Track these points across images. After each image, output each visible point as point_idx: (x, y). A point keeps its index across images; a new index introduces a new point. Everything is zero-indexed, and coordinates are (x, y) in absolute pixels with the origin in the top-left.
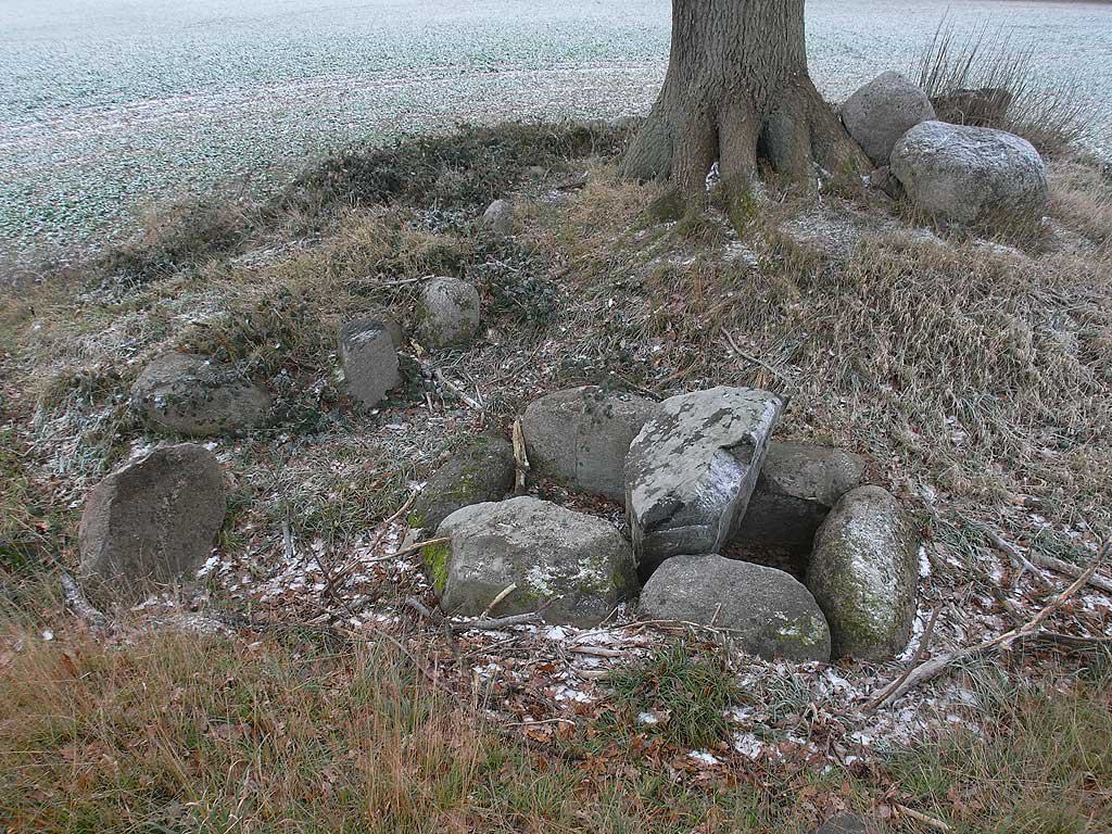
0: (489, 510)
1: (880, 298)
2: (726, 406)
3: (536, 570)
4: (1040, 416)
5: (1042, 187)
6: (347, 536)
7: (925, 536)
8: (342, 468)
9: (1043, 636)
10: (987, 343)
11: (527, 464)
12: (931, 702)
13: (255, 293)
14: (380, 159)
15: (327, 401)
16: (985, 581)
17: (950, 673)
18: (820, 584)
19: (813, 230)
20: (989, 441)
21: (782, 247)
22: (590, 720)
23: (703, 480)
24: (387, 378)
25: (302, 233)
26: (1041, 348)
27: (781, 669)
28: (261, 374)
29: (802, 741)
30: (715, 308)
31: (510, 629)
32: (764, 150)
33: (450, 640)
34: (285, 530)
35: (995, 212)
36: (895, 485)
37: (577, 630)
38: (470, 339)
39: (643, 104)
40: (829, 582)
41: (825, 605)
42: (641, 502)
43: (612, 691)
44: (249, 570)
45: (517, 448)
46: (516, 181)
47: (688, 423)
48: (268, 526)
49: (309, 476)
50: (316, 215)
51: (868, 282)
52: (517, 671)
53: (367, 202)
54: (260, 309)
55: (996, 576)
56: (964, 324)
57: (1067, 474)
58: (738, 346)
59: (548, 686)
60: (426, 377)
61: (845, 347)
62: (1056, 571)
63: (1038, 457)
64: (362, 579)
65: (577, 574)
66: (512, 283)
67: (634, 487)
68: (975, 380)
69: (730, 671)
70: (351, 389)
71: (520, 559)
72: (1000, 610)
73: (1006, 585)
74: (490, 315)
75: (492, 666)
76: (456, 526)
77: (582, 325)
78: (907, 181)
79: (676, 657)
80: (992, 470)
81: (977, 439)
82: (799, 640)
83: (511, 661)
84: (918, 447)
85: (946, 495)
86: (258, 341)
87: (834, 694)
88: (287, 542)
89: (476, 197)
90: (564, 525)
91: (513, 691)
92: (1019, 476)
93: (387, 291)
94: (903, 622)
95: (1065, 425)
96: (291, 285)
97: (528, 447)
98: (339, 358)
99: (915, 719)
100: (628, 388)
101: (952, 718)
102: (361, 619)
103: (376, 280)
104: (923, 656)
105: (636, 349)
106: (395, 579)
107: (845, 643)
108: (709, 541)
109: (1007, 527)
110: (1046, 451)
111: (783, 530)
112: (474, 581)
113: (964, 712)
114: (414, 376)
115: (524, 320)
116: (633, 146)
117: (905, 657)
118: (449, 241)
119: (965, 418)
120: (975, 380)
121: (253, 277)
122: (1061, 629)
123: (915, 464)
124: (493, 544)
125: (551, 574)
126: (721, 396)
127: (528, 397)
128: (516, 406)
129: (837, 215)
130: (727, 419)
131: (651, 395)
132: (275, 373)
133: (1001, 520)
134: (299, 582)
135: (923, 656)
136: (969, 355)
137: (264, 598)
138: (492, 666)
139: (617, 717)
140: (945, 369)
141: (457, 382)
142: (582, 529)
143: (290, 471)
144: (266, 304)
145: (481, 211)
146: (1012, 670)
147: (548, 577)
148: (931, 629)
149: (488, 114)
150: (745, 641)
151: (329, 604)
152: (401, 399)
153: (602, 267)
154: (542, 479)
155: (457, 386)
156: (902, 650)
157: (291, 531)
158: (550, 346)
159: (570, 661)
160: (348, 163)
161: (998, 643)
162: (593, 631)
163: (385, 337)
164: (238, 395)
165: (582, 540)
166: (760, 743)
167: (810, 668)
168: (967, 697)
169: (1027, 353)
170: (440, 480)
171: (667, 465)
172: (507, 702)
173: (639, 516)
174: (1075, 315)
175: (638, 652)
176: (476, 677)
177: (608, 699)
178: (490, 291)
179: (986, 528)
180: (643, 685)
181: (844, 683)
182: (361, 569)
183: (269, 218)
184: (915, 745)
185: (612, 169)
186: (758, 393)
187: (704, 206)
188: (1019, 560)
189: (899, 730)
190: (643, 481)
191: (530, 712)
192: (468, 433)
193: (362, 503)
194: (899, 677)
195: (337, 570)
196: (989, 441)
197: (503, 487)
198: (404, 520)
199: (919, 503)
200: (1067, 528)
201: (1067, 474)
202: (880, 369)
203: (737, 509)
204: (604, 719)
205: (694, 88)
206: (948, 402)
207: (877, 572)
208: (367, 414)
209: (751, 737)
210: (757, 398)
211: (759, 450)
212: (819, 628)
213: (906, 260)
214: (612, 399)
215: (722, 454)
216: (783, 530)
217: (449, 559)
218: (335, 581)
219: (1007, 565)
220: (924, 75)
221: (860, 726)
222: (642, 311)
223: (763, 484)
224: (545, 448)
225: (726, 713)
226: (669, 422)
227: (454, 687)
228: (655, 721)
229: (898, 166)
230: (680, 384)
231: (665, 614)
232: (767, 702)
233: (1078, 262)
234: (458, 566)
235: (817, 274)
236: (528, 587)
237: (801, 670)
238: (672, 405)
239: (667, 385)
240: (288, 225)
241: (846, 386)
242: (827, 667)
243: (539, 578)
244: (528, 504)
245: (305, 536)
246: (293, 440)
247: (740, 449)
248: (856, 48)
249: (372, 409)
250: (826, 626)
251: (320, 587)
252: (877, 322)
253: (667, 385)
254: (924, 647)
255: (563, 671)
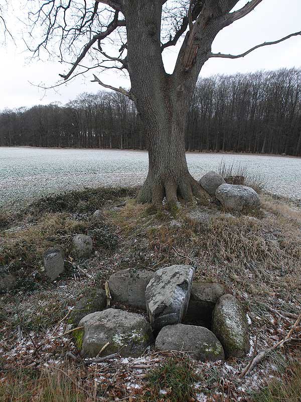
0: (98, 314)
1: (219, 234)
2: (177, 271)
3: (116, 336)
4: (273, 267)
5: (259, 200)
6: (44, 330)
7: (247, 310)
8: (42, 303)
9: (292, 340)
10: (252, 245)
11: (111, 297)
12: (262, 371)
13: (13, 241)
14: (59, 198)
15: (38, 278)
16: (270, 323)
17: (266, 359)
18: (217, 330)
19: (196, 215)
20: (260, 276)
21: (188, 221)
22: (141, 396)
23: (173, 296)
24: (59, 269)
25: (32, 221)
26: (269, 246)
27: (208, 365)
28: (14, 269)
29: (221, 393)
30: (169, 240)
31: (108, 361)
32: (179, 193)
33: (84, 368)
34: (19, 329)
35: (247, 208)
36: (235, 294)
37: (133, 358)
38: (88, 255)
39: (142, 182)
40: (219, 330)
41: (219, 338)
42: (152, 307)
43: (148, 383)
44: (3, 346)
45: (107, 292)
46: (103, 204)
47: (165, 278)
48: (12, 327)
49: (30, 307)
50: (37, 215)
51: (215, 230)
52: (111, 378)
53: (54, 211)
54: (15, 246)
55: (272, 321)
56: (246, 241)
57: (285, 284)
58: (178, 252)
59: (124, 383)
60: (74, 268)
61: (211, 250)
62: (290, 317)
63: (276, 280)
64: (49, 346)
65: (131, 336)
66: (104, 236)
67: (149, 302)
68: (252, 257)
69: (191, 368)
70: (47, 274)
71: (110, 332)
72: (276, 333)
73: (276, 324)
74: (96, 247)
75: (101, 377)
76: (86, 322)
77: (127, 248)
78: (221, 200)
79: (171, 365)
80: (263, 285)
81: (256, 276)
82: (213, 353)
83: (109, 374)
84: (239, 280)
85: (251, 295)
86: (13, 258)
87: (228, 372)
88: (19, 333)
89: (91, 209)
90: (126, 318)
91: (111, 387)
92: (272, 287)
93: (61, 240)
94: (247, 341)
95: (281, 269)
96: (26, 238)
97: (111, 291)
98: (43, 263)
99: (258, 378)
100: (144, 268)
101: (271, 376)
102: (48, 363)
103: (57, 236)
104: (256, 354)
105: (145, 255)
106: (62, 345)
107: (230, 352)
108: (177, 319)
109: (272, 304)
110: (277, 277)
111: (201, 312)
112: (93, 343)
113: (273, 372)
114: (70, 268)
115: (108, 247)
116: (140, 192)
117: (250, 354)
118: (81, 223)
119: (251, 269)
120: (252, 257)
121: (13, 236)
122: (297, 337)
123: (239, 285)
124: (100, 327)
125: (122, 337)
126: (175, 268)
127: (110, 273)
128: (106, 277)
129: (203, 211)
130: (178, 275)
131: (152, 270)
132: (19, 269)
133: (269, 302)
134: (23, 350)
135: (256, 354)
136: (249, 250)
137: (8, 358)
138: (101, 377)
139: (152, 393)
140: (242, 254)
141: (85, 270)
142: (135, 319)
143: (22, 306)
144: (17, 245)
145: (92, 214)
146: (286, 355)
147: (121, 338)
148: (256, 342)
149: (94, 185)
150: (195, 355)
151: (36, 358)
152: (65, 277)
153: (132, 230)
154: (117, 302)
155: (85, 271)
156: (248, 352)
157: (21, 329)
158: (116, 256)
159: (132, 372)
160: (48, 199)
161: (279, 345)
162: (139, 358)
163: (60, 255)
164: (3, 277)
165: (132, 323)
166: (206, 397)
167: (219, 363)
168: (274, 367)
169: (264, 247)
170: (79, 305)
171: (160, 293)
172: (108, 392)
173: (152, 312)
174: (276, 235)
175: (156, 365)
176: (95, 383)
177: (148, 386)
178: (96, 239)
179: (266, 305)
180: (158, 378)
181: (232, 368)
182: (49, 343)
183: (20, 217)
184: (261, 389)
185: (133, 200)
186: (187, 266)
187: (162, 210)
188: (278, 315)
189: (254, 384)
190: (152, 299)
191: (117, 396)
192: (89, 287)
193: (50, 316)
194: (249, 363)
195: (39, 344)
196: (260, 276)
197: (103, 307)
198: (66, 322)
199: (243, 299)
200: (290, 302)
201: (285, 284)
202: (223, 256)
203: (185, 306)
204: (147, 395)
205: (156, 176)
206: (245, 265)
207: (235, 324)
208: (52, 282)
209: (202, 395)
210: (186, 268)
211: (189, 285)
212: (219, 347)
213: (225, 222)
214: (139, 272)
215: (178, 287)
216: (201, 312)
217: (84, 335)
218: (38, 348)
219: (275, 317)
220: (220, 173)
221: (240, 384)
222: (146, 243)
223: (192, 298)
224: (116, 291)
225: (192, 386)
226: (159, 278)
227: (86, 388)
228: (166, 393)
229: (218, 196)
230: (161, 266)
231: (164, 349)
232: (206, 379)
233: (273, 221)
234: (87, 337)
235: (200, 229)
236: (114, 343)
237: (216, 365)
238: (159, 272)
239: (157, 266)
240: (26, 219)
241: (213, 263)
242: (224, 362)
243: (118, 339)
244: (112, 311)
245: (27, 330)
246: (24, 293)
247: (183, 285)
248: (200, 166)
249: (54, 281)
250: (221, 346)
251: (32, 351)
252: (220, 242)
253: (157, 266)
254: (255, 351)
255: (129, 376)
